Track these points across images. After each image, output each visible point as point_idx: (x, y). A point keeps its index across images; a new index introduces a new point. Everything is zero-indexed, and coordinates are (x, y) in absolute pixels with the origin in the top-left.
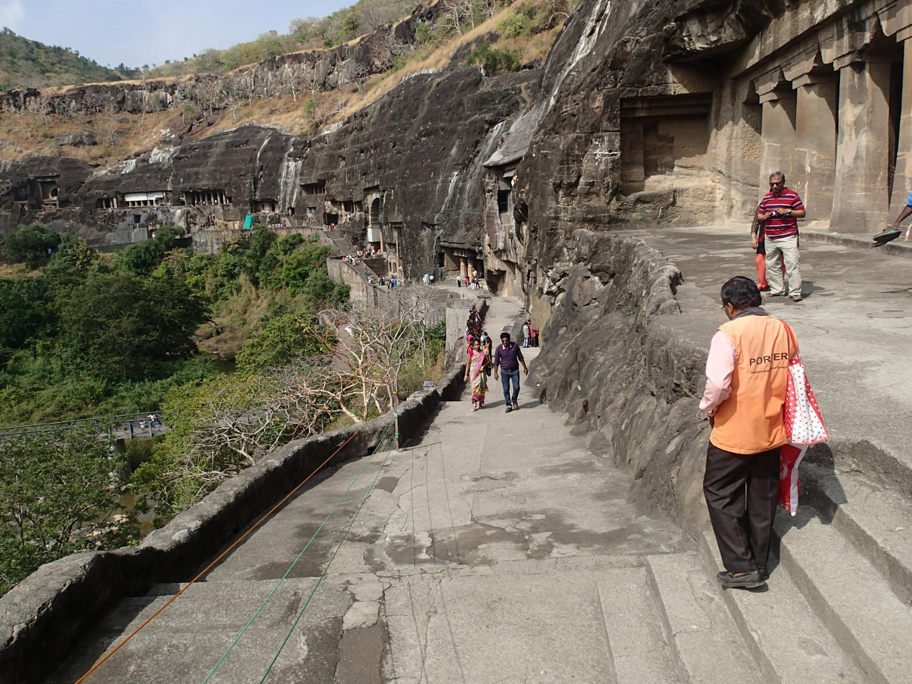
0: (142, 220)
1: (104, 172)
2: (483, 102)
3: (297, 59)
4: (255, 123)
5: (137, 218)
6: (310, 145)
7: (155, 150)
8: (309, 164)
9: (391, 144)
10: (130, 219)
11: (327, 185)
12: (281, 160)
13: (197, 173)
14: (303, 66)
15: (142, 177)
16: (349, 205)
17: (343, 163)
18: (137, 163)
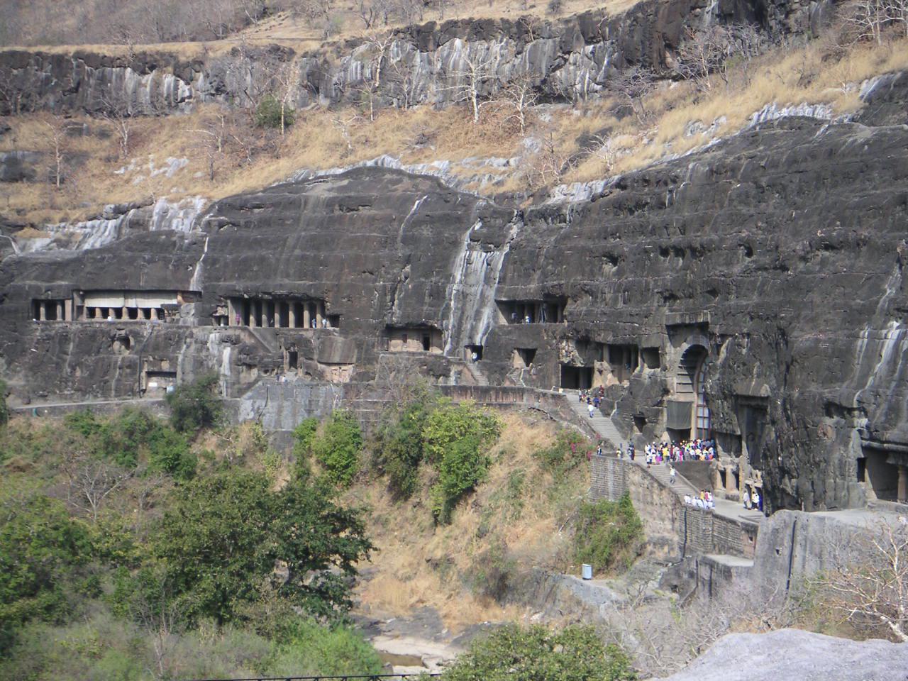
11: (570, 307)
12: (456, 244)
16: (624, 355)
17: (609, 268)
18: (118, 229)
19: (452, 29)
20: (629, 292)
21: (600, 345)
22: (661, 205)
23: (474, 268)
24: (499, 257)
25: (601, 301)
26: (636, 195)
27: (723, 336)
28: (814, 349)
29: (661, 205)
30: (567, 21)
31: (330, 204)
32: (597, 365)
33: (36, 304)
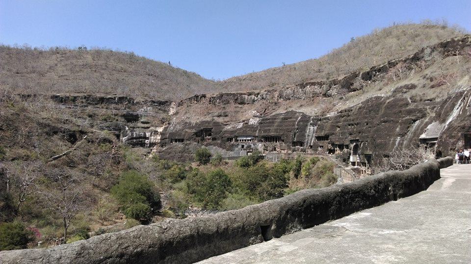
0: (245, 147)
1: (229, 127)
2: (410, 112)
3: (313, 84)
4: (294, 110)
5: (243, 146)
6: (320, 120)
7: (251, 120)
8: (321, 128)
9: (366, 124)
11: (330, 137)
12: (307, 125)
13: (269, 130)
14: (316, 87)
15: (245, 130)
17: (338, 129)
18: (243, 125)
20: (343, 134)
23: (311, 129)
24: (316, 128)
32: (336, 149)
33: (228, 139)
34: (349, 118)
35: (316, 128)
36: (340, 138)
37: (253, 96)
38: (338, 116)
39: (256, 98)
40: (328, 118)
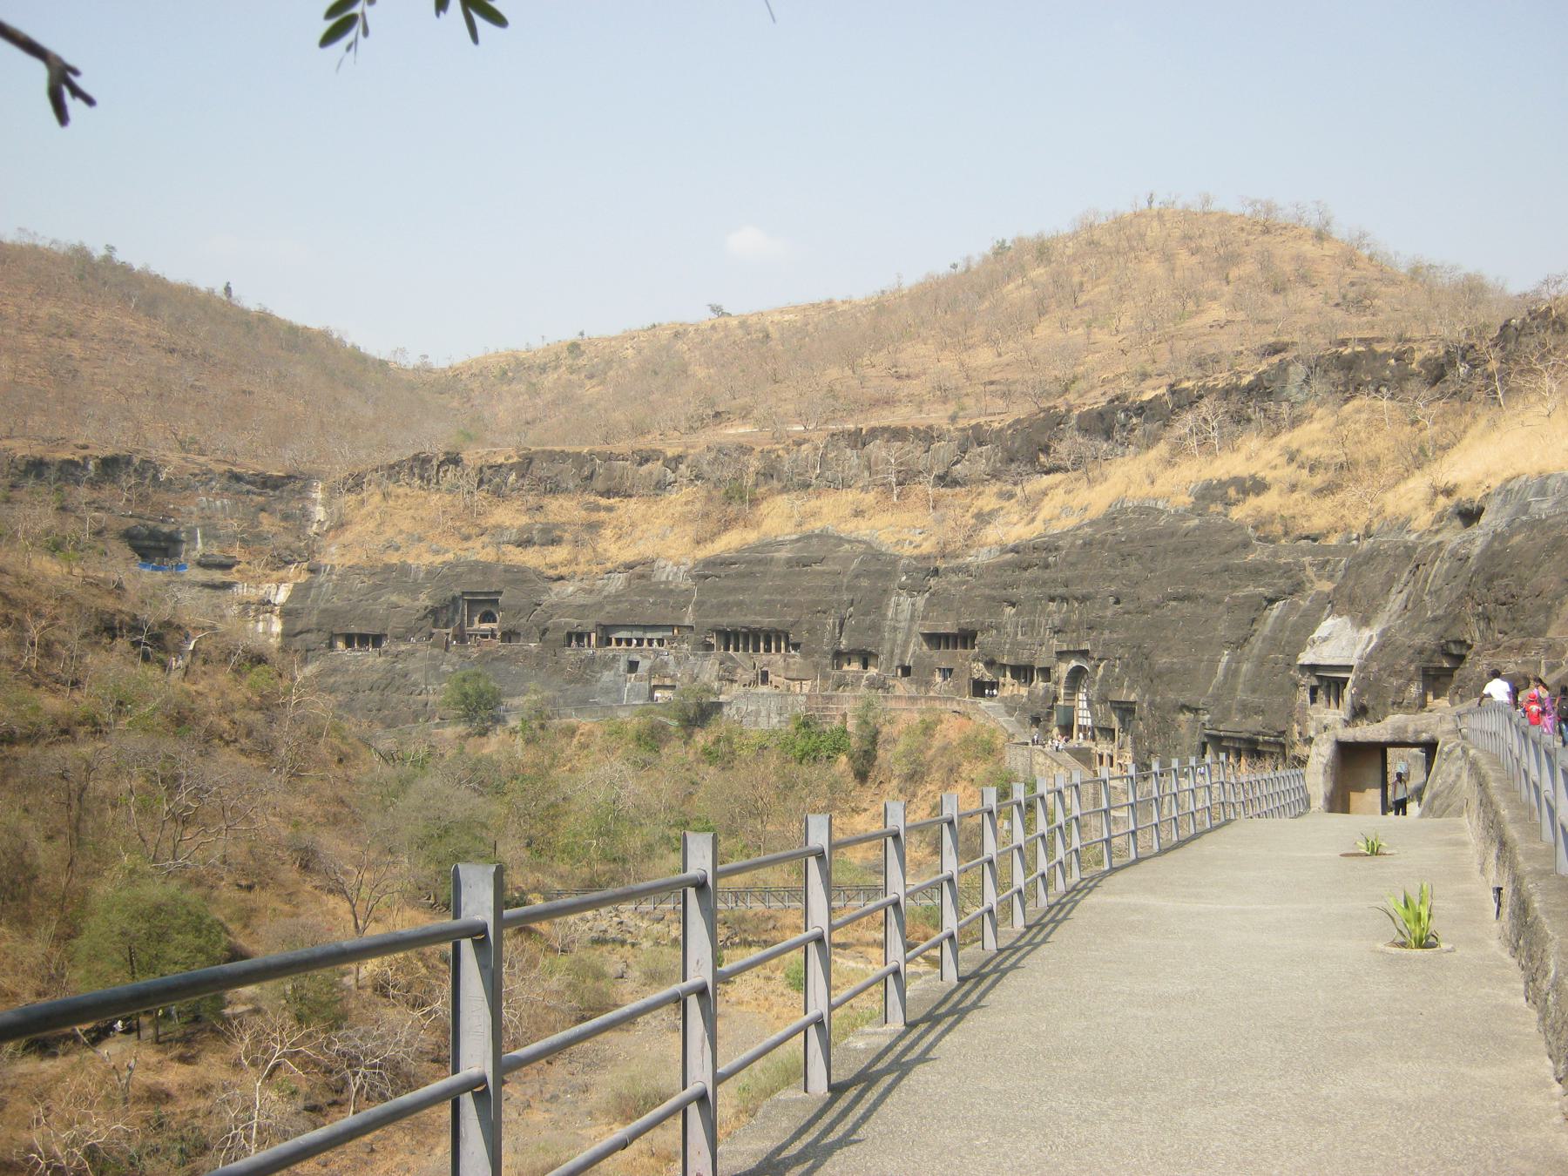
5: (633, 666)
8: (938, 601)
10: (622, 666)
11: (980, 638)
13: (740, 604)
16: (1023, 672)
17: (1010, 611)
18: (629, 581)
19: (874, 433)
21: (1004, 666)
22: (1047, 566)
23: (902, 607)
24: (921, 601)
25: (1009, 632)
26: (1024, 557)
27: (1101, 660)
28: (1170, 670)
29: (1047, 566)
30: (963, 430)
31: (789, 562)
33: (570, 635)
34: (1047, 574)
35: (921, 601)
36: (1019, 644)
37: (655, 467)
38: (1009, 564)
39: (671, 476)
40: (964, 569)
